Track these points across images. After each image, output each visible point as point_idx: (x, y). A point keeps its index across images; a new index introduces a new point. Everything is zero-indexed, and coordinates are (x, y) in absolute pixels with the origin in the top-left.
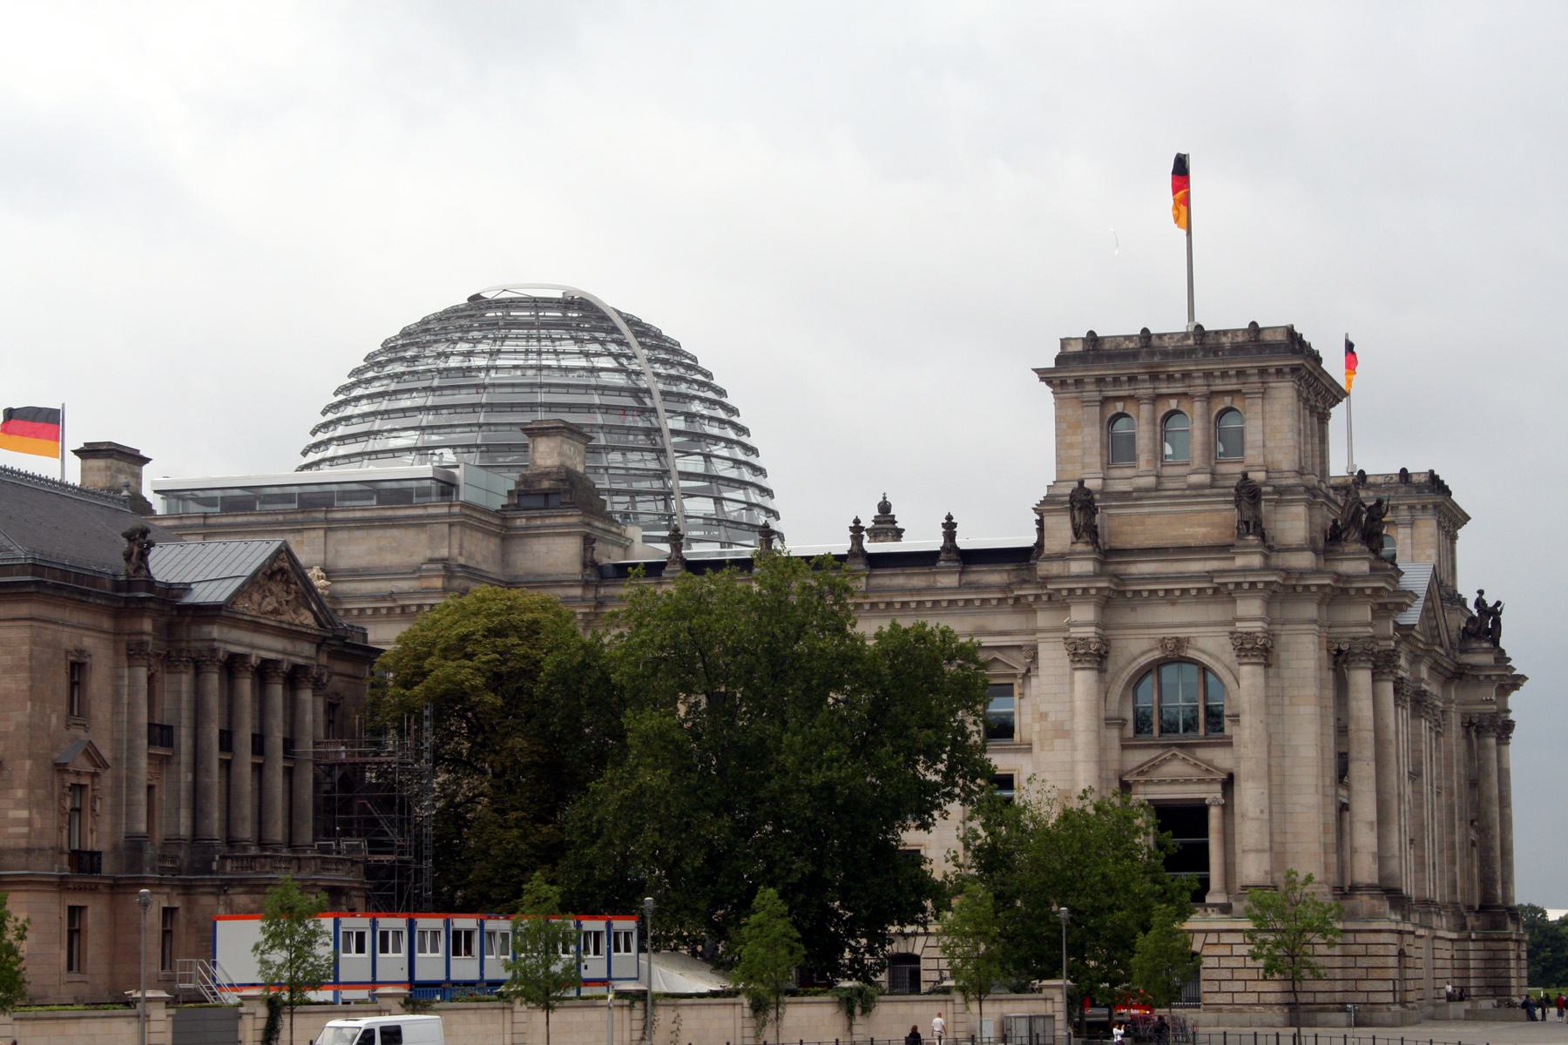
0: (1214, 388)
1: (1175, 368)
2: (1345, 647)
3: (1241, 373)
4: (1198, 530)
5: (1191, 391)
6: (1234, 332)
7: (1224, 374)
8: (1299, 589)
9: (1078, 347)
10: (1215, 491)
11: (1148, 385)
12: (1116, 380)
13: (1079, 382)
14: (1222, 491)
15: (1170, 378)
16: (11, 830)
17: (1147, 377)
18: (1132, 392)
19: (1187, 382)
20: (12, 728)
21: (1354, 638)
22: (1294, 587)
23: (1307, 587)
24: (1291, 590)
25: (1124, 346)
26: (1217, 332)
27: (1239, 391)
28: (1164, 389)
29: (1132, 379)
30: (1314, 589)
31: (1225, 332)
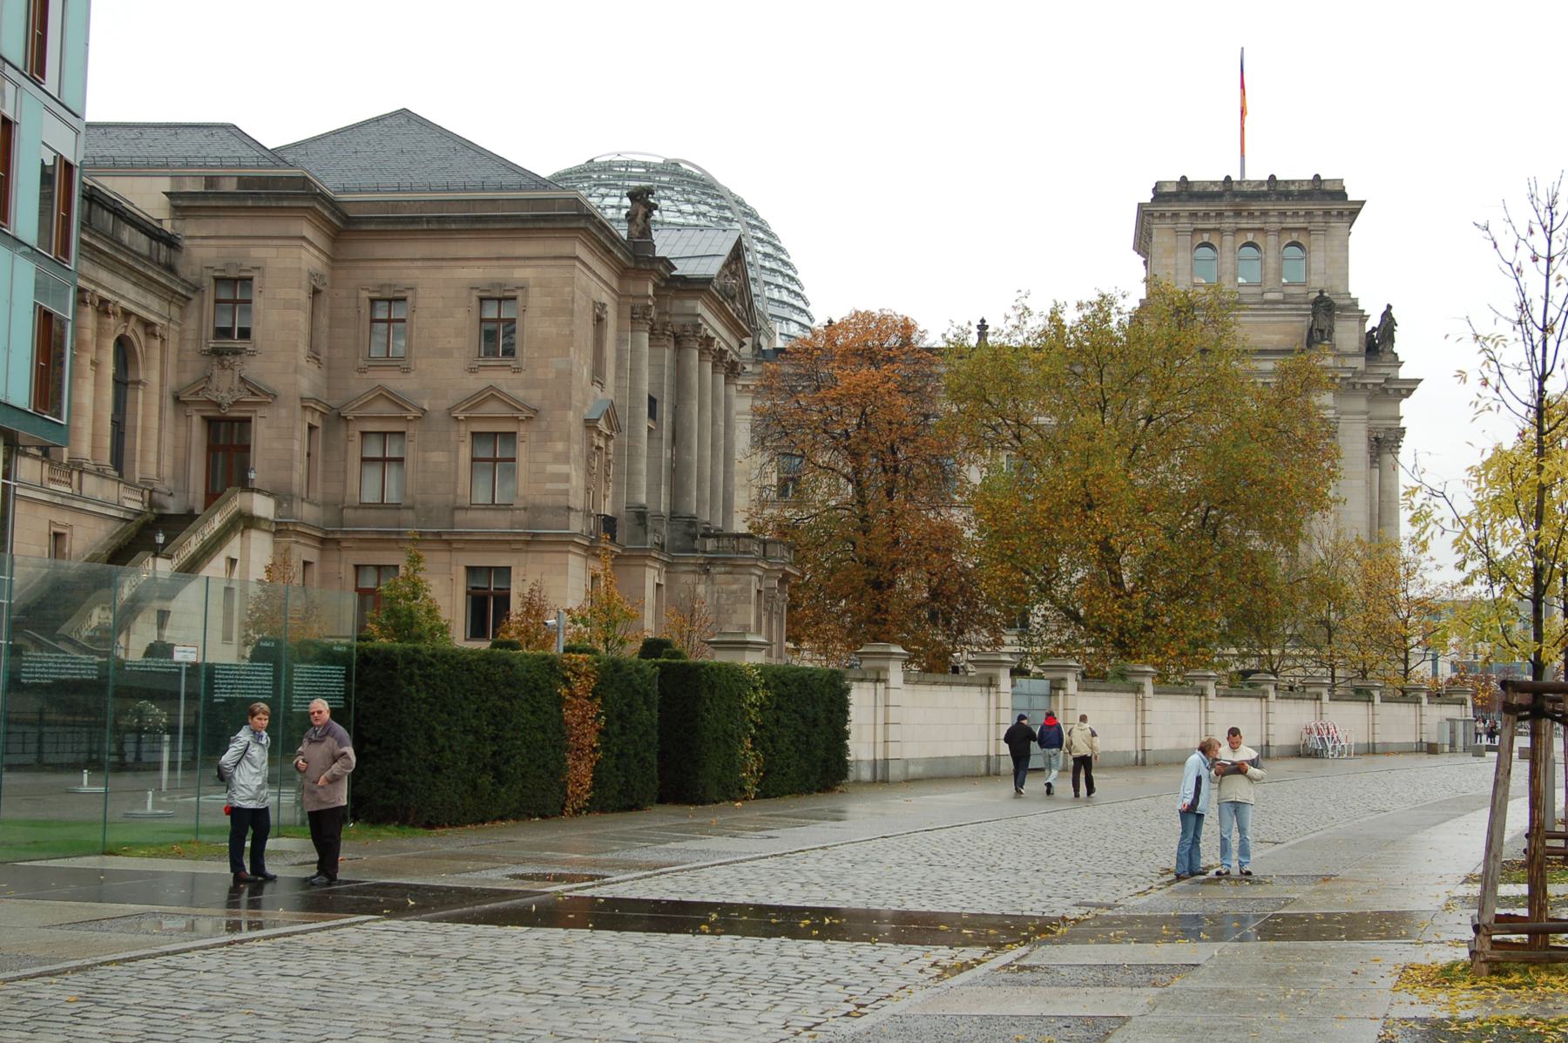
0: (1284, 225)
1: (1255, 207)
2: (1381, 436)
3: (1309, 213)
4: (1273, 337)
5: (1267, 226)
6: (1301, 182)
7: (1296, 214)
8: (1358, 386)
9: (1173, 189)
10: (1288, 306)
11: (1231, 220)
12: (1207, 215)
13: (1175, 215)
14: (1294, 306)
15: (1251, 214)
16: (549, 486)
17: (1232, 214)
18: (1218, 226)
19: (1263, 219)
20: (551, 376)
21: (1390, 429)
22: (1354, 385)
23: (1364, 385)
24: (1351, 387)
25: (1210, 189)
26: (1286, 182)
27: (1305, 229)
28: (1244, 223)
29: (1220, 214)
30: (1370, 387)
31: (1293, 182)
